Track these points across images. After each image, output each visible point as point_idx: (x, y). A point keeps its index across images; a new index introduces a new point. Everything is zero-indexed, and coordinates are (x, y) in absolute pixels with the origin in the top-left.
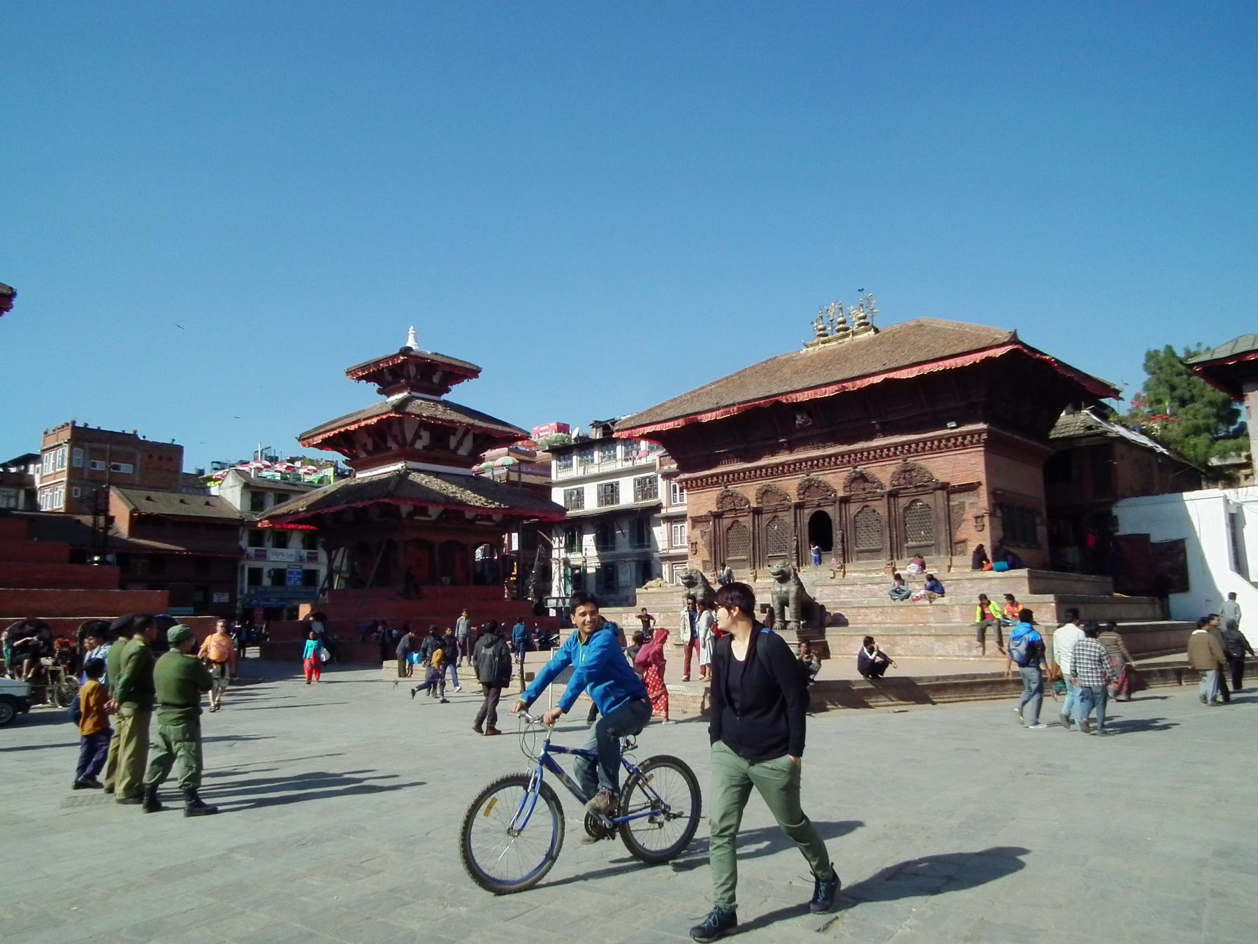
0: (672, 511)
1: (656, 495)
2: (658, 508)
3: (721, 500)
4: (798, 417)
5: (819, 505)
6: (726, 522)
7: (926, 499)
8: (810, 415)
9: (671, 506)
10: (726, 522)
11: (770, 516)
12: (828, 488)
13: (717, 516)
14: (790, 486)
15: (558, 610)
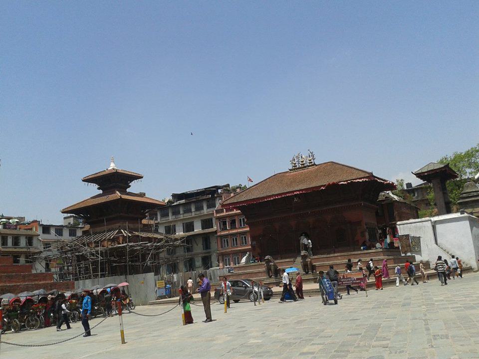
8: (299, 198)
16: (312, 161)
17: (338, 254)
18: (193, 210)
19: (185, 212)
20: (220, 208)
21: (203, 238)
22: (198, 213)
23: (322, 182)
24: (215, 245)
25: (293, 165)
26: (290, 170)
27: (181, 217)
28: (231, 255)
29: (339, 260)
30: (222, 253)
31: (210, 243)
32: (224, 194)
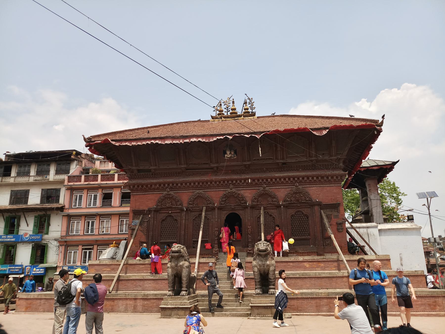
0: (71, 212)
1: (58, 201)
2: (62, 209)
3: (161, 201)
4: (228, 152)
5: (233, 209)
6: (162, 216)
7: (306, 211)
8: (235, 153)
9: (71, 207)
10: (162, 216)
11: (197, 214)
12: (243, 198)
13: (157, 211)
14: (216, 196)
15: (31, 280)
16: (250, 110)
17: (307, 258)
18: (33, 172)
19: (19, 174)
20: (77, 174)
21: (36, 217)
22: (39, 178)
23: (295, 125)
24: (56, 228)
25: (218, 112)
26: (213, 117)
27: (11, 180)
28: (80, 247)
29: (305, 268)
30: (66, 242)
31: (49, 225)
32: (86, 160)
